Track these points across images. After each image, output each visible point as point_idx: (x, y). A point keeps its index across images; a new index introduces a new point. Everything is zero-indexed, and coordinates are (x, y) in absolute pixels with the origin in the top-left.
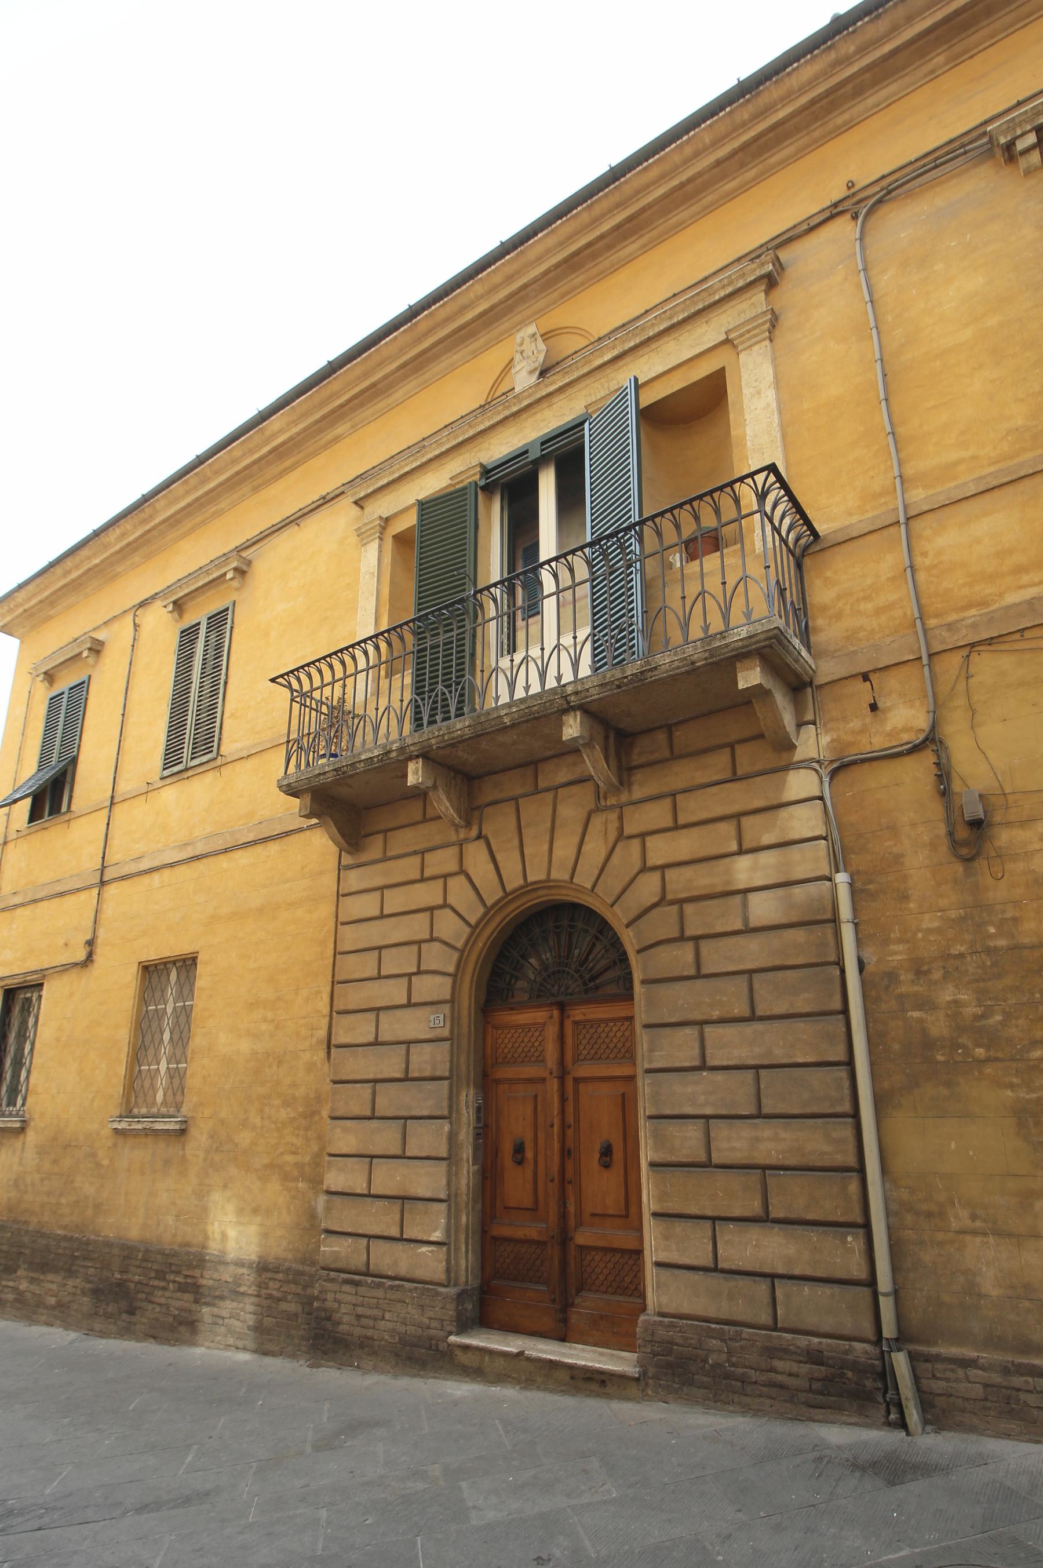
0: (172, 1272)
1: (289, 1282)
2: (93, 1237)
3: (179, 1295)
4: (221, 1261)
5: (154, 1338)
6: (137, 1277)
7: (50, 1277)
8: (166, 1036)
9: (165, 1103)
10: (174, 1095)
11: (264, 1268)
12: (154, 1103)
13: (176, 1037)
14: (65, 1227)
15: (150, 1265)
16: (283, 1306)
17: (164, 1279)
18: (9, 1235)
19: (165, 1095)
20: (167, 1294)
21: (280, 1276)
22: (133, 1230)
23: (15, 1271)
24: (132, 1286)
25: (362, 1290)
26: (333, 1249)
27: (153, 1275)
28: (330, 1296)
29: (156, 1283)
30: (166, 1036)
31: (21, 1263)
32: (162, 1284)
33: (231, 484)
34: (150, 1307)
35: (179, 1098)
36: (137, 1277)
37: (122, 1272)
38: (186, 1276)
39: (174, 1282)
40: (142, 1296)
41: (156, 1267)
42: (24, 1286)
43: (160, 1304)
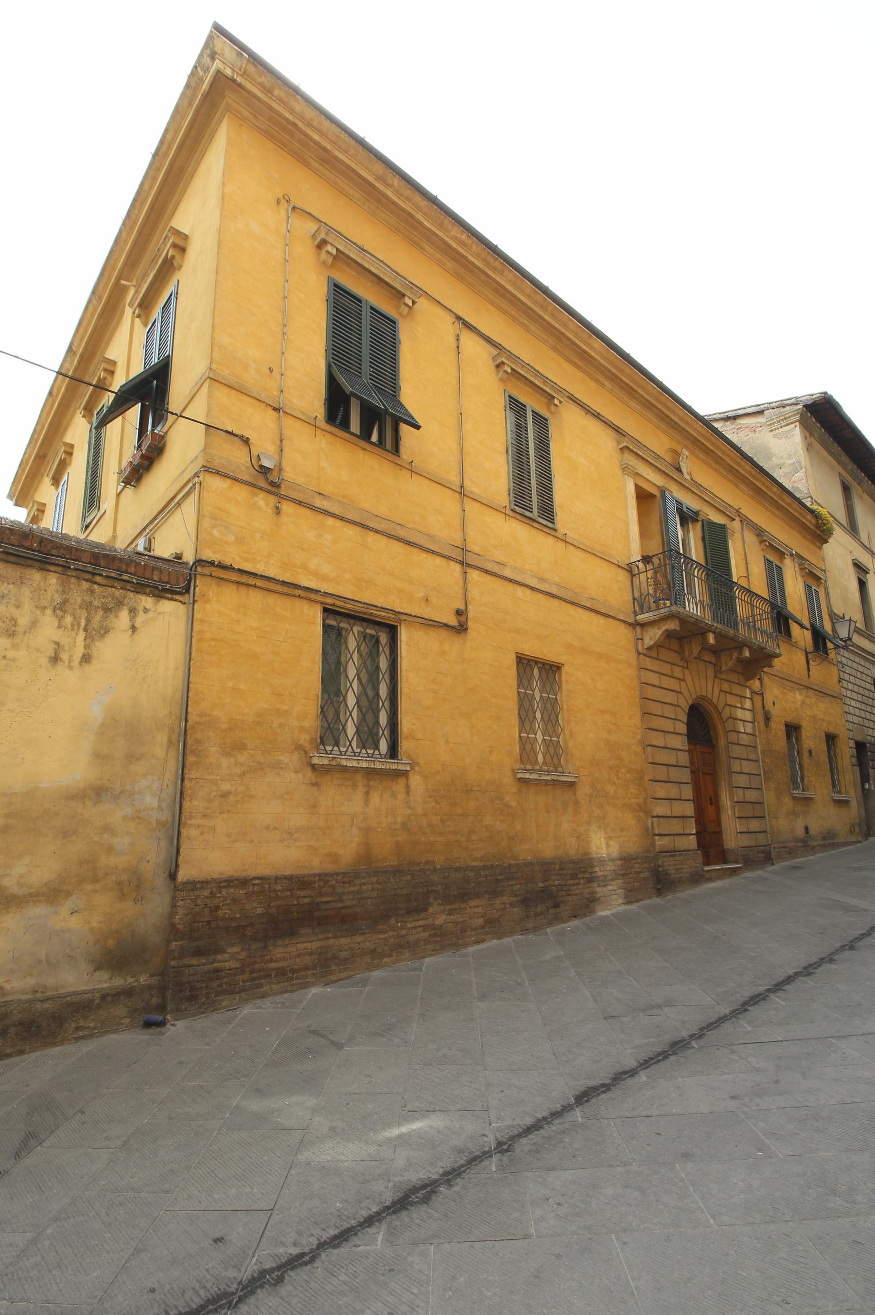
0: (582, 872)
1: (643, 863)
2: (512, 862)
3: (588, 885)
4: (602, 862)
5: (575, 917)
6: (557, 882)
7: (472, 903)
8: (538, 715)
9: (545, 763)
10: (552, 758)
11: (626, 860)
12: (536, 762)
13: (546, 717)
14: (481, 859)
15: (565, 872)
16: (642, 875)
17: (577, 878)
18: (409, 877)
19: (544, 758)
20: (580, 887)
21: (639, 861)
22: (548, 850)
23: (426, 910)
24: (554, 888)
25: (677, 858)
26: (660, 842)
27: (569, 877)
28: (666, 864)
29: (572, 882)
30: (538, 715)
31: (431, 900)
32: (576, 881)
33: (549, 329)
34: (570, 898)
35: (556, 761)
36: (557, 882)
37: (544, 882)
38: (591, 873)
39: (583, 878)
40: (561, 893)
41: (570, 872)
42: (441, 920)
43: (576, 895)
